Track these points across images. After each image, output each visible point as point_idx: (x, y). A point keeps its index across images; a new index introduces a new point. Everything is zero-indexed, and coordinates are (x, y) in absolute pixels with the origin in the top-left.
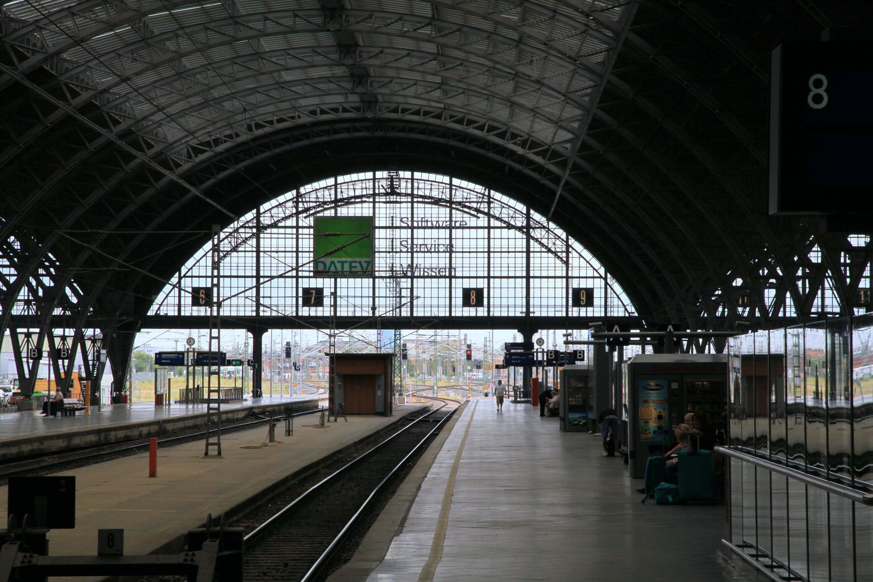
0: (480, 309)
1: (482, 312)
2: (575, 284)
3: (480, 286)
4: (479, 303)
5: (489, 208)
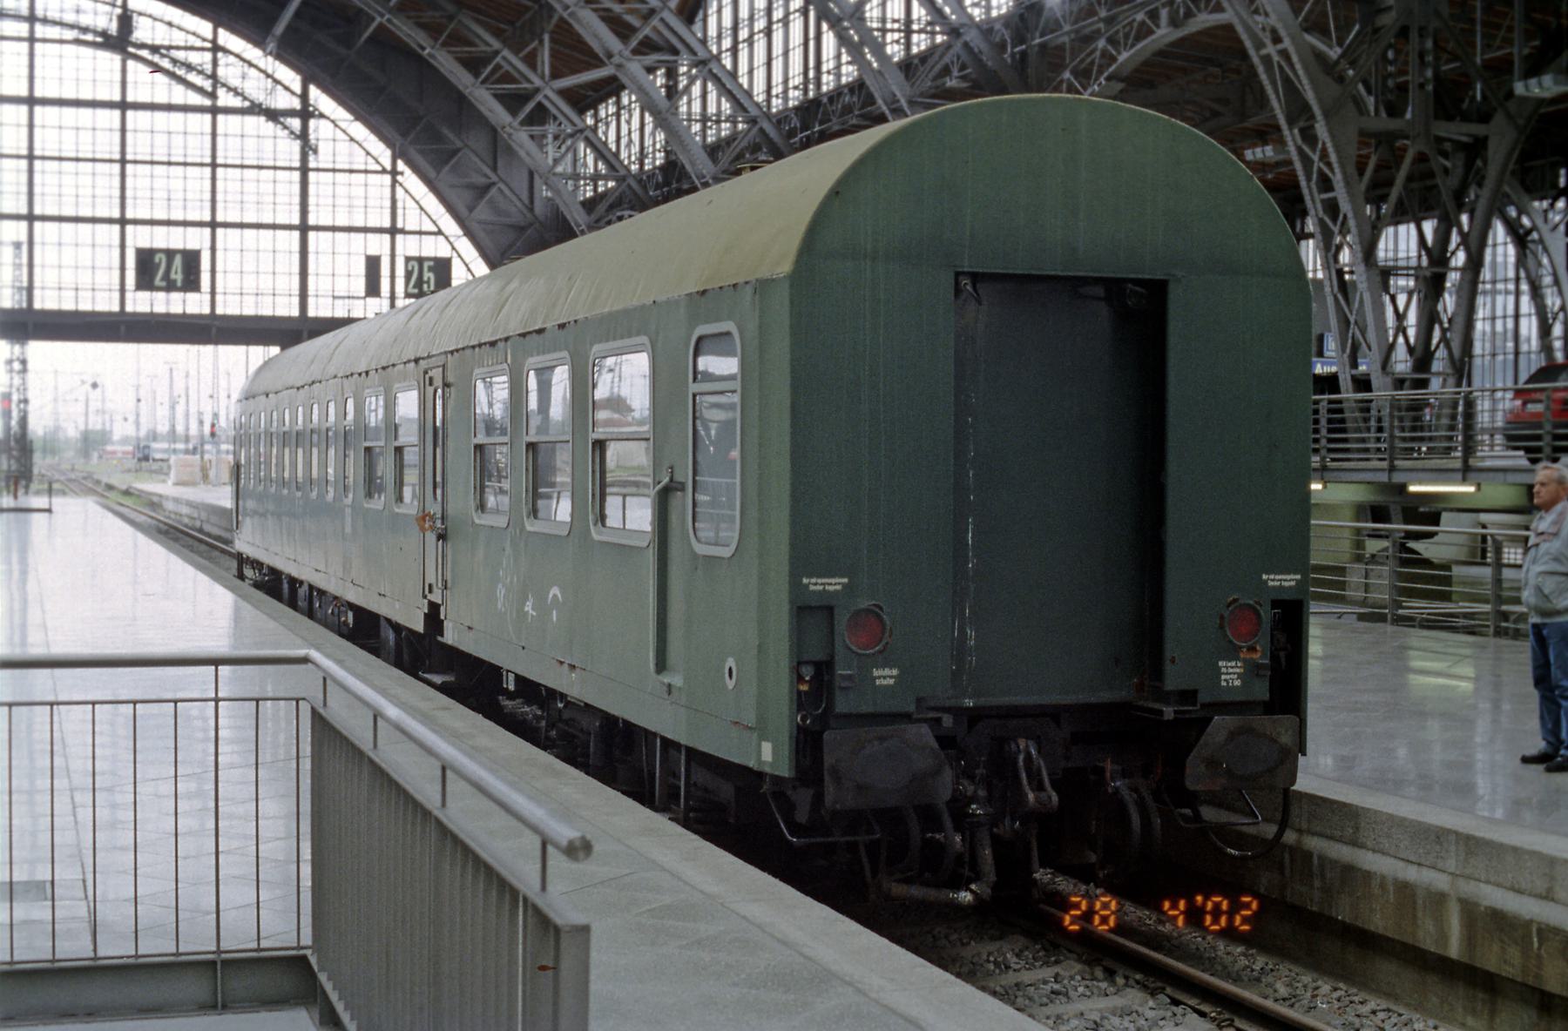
0: (192, 297)
1: (194, 304)
2: (409, 246)
3: (191, 246)
4: (191, 284)
5: (215, 63)
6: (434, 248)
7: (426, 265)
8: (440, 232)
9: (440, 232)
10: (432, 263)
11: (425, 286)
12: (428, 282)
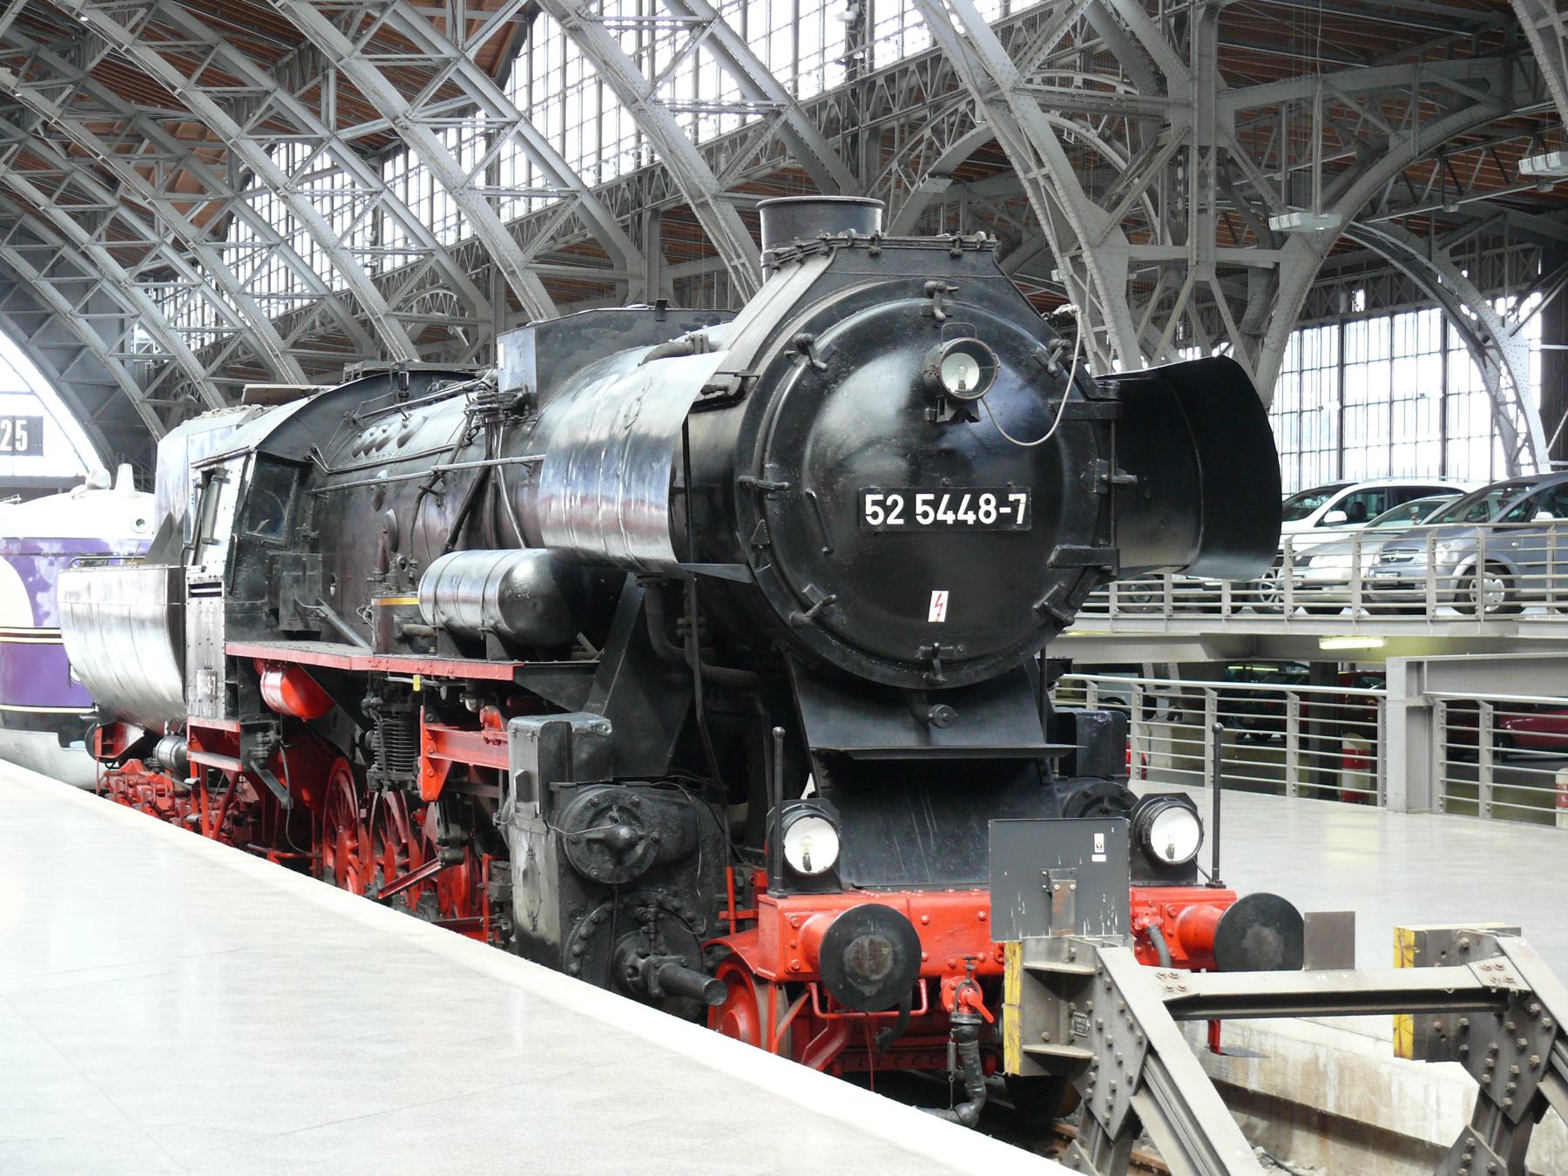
6: (27, 408)
7: (19, 423)
8: (32, 392)
9: (32, 392)
10: (25, 422)
11: (18, 444)
12: (21, 440)
